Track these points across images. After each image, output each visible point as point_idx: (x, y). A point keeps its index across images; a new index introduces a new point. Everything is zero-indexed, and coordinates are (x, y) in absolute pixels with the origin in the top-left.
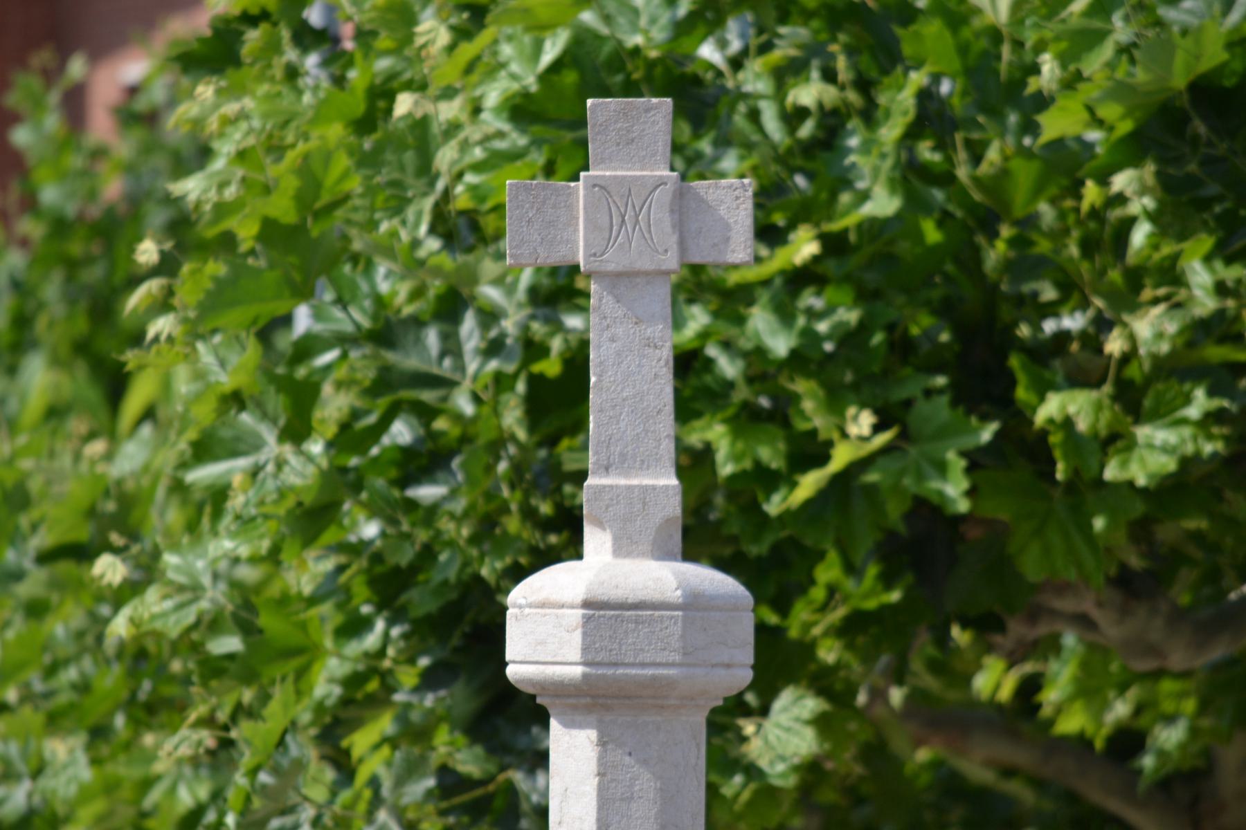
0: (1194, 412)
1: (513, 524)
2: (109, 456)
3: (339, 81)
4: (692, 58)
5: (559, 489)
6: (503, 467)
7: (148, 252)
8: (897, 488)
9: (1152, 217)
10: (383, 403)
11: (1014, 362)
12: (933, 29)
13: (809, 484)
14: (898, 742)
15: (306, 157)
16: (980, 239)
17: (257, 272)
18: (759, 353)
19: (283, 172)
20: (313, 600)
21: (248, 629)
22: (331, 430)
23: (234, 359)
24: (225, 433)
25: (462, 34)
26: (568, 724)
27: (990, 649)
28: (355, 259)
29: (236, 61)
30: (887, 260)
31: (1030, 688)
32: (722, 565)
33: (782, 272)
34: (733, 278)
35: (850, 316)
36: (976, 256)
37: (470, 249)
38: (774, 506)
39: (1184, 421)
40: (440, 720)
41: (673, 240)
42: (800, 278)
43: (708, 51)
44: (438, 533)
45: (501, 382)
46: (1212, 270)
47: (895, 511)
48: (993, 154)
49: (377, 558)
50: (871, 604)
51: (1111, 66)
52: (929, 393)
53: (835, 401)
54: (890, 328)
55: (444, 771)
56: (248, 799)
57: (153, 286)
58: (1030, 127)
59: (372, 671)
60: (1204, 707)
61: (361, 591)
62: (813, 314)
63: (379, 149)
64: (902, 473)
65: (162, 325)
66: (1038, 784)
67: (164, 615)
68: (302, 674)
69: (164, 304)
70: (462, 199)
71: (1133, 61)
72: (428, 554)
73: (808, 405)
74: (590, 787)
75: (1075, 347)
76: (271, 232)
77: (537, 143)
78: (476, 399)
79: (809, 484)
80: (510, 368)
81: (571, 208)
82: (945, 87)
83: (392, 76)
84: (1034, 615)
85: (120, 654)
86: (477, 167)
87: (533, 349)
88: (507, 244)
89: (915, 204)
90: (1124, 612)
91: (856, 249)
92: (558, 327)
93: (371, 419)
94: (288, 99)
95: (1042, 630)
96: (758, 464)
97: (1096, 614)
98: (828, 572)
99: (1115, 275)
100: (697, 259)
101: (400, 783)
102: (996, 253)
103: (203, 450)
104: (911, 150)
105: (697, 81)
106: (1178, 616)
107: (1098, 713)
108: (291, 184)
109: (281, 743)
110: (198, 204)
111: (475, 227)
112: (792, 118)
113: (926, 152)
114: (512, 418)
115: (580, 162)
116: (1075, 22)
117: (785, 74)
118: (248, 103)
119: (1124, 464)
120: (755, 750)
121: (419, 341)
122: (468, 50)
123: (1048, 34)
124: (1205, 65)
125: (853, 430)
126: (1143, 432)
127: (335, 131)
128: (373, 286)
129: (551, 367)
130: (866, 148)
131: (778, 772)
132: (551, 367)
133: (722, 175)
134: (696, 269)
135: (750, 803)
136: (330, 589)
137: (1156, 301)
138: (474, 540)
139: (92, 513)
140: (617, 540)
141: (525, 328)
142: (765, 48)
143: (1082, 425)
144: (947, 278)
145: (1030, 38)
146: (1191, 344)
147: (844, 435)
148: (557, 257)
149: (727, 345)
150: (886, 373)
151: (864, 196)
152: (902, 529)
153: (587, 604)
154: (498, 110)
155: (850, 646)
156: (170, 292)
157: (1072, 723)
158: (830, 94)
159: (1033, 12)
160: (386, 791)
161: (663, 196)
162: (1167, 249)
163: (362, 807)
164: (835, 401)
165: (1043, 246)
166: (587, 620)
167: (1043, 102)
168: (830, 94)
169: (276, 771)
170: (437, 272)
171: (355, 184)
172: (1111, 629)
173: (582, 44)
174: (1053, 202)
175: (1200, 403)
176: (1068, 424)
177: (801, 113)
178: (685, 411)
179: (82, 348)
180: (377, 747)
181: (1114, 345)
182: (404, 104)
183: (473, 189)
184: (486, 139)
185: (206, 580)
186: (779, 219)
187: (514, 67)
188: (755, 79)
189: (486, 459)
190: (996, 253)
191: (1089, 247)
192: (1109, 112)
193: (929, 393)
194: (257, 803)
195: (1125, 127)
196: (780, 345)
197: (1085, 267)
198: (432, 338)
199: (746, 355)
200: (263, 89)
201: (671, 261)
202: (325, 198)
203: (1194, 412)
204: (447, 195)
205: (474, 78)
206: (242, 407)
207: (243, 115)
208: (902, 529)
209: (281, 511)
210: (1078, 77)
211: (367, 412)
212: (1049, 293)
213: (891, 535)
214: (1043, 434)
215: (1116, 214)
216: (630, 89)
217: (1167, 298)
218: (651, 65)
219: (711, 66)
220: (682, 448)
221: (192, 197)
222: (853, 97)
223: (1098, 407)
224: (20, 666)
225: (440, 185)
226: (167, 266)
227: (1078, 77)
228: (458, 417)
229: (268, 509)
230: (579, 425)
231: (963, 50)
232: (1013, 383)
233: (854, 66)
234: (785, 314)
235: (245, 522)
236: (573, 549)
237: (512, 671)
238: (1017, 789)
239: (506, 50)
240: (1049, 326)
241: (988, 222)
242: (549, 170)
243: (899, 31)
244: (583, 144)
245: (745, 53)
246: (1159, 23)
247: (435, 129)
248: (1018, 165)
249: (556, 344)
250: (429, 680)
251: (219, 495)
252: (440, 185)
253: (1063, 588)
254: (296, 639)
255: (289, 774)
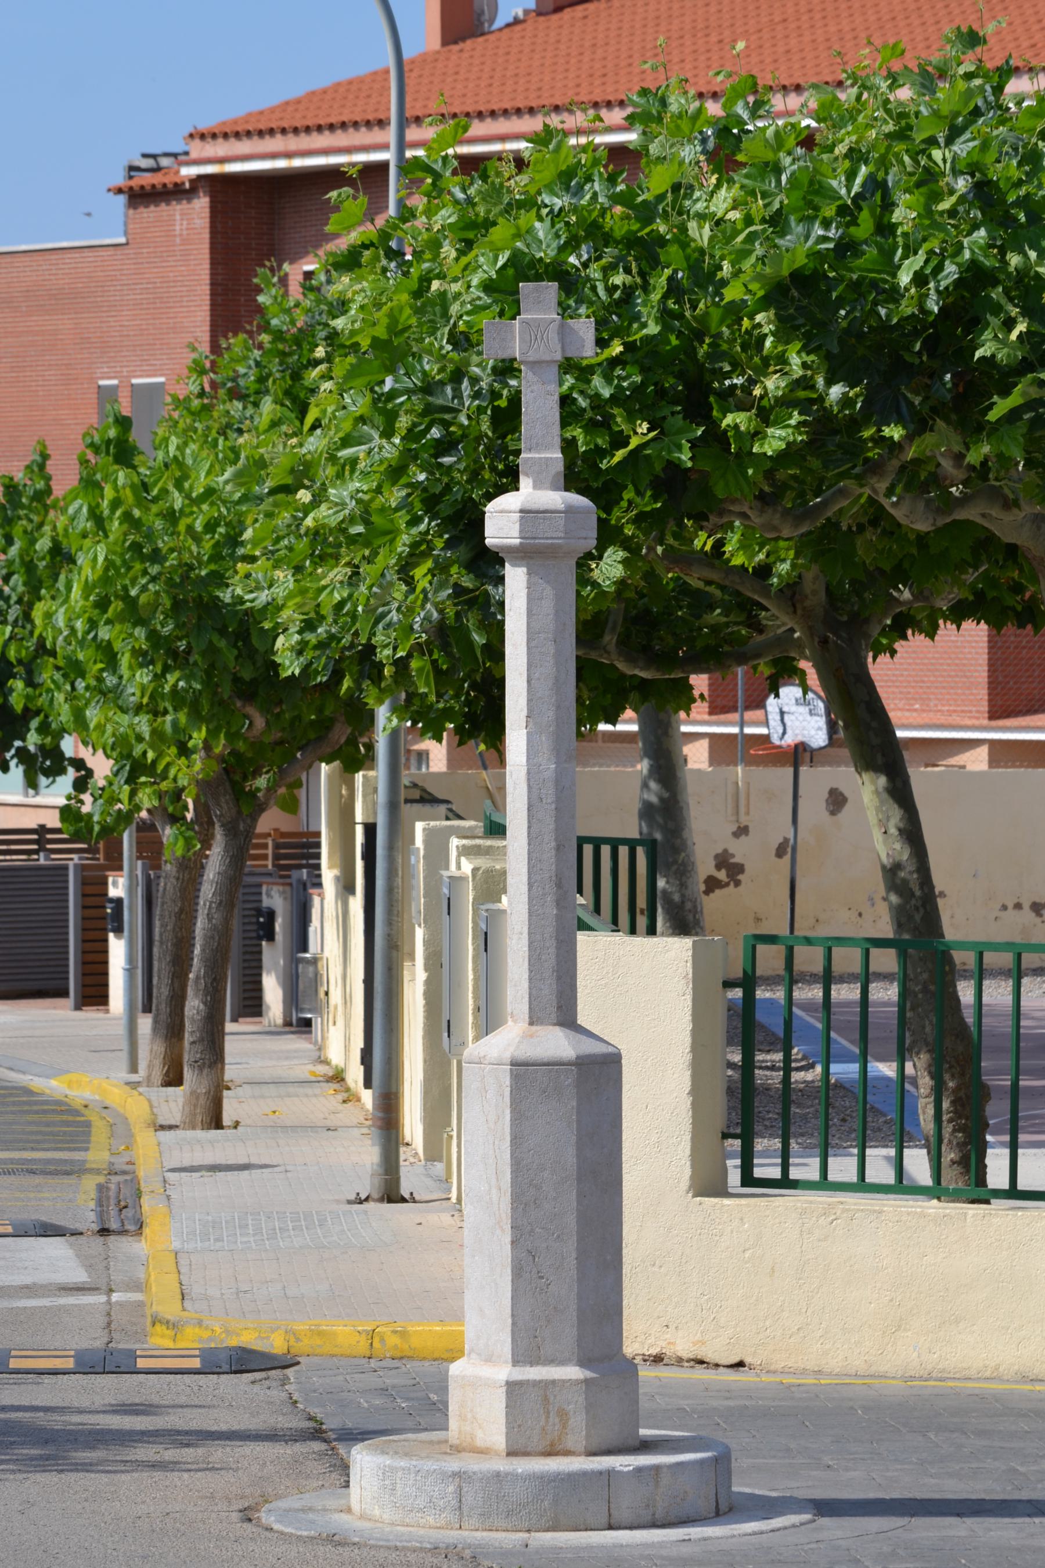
0: (793, 422)
1: (487, 475)
2: (301, 445)
3: (406, 274)
4: (566, 263)
5: (507, 458)
6: (481, 447)
7: (320, 352)
8: (659, 456)
9: (773, 334)
10: (427, 420)
11: (712, 399)
12: (674, 249)
13: (620, 455)
14: (659, 570)
15: (391, 309)
16: (696, 344)
17: (370, 360)
18: (598, 395)
19: (381, 316)
20: (397, 509)
21: (367, 523)
22: (404, 432)
23: (360, 401)
24: (356, 434)
25: (462, 253)
26: (513, 565)
27: (702, 528)
28: (414, 355)
29: (359, 265)
30: (654, 354)
31: (719, 544)
32: (580, 492)
33: (607, 359)
34: (585, 363)
35: (638, 379)
36: (694, 350)
37: (465, 350)
38: (603, 466)
39: (789, 426)
40: (454, 562)
41: (559, 347)
42: (615, 362)
43: (572, 260)
44: (453, 478)
45: (480, 410)
46: (800, 357)
47: (658, 467)
48: (701, 305)
49: (425, 490)
50: (648, 509)
51: (754, 266)
52: (673, 413)
53: (631, 418)
54: (656, 384)
55: (456, 585)
56: (368, 599)
57: (323, 367)
58: (718, 293)
59: (423, 541)
60: (797, 556)
61: (418, 505)
62: (619, 377)
63: (424, 305)
64: (662, 449)
65: (327, 385)
66: (722, 588)
67: (329, 516)
68: (392, 541)
69: (327, 377)
70: (462, 326)
71: (764, 264)
72: (448, 488)
73: (619, 420)
74: (524, 593)
75: (738, 392)
76: (376, 343)
77: (495, 301)
78: (469, 417)
79: (620, 455)
80: (485, 404)
81: (513, 332)
82: (680, 275)
83: (430, 271)
84: (721, 513)
85: (306, 534)
86: (468, 313)
87: (495, 395)
88: (484, 347)
89: (666, 328)
90: (762, 512)
91: (640, 348)
92: (507, 385)
93: (423, 427)
94: (382, 283)
95: (725, 520)
96: (596, 445)
97: (749, 513)
98: (628, 494)
99: (757, 359)
100: (569, 355)
101: (436, 592)
102: (703, 350)
103: (346, 442)
104: (664, 304)
105: (568, 273)
106: (786, 513)
107: (751, 558)
108: (385, 321)
109: (383, 575)
110: (343, 330)
111: (468, 339)
112: (611, 289)
113: (671, 304)
114: (485, 426)
115: (515, 310)
116: (738, 246)
117: (608, 270)
118: (365, 284)
119: (762, 446)
120: (596, 574)
121: (443, 392)
122: (464, 260)
123: (726, 252)
124: (796, 266)
125: (639, 431)
126: (770, 431)
127: (404, 297)
128: (422, 367)
129: (503, 403)
130: (645, 304)
131: (607, 585)
132: (503, 403)
133: (580, 316)
134: (568, 359)
135: (594, 599)
136: (405, 504)
137: (776, 372)
138: (468, 481)
139: (292, 471)
140: (534, 482)
141: (491, 385)
142: (598, 258)
143: (743, 428)
144: (680, 360)
145: (718, 254)
146: (791, 391)
147: (636, 433)
148: (506, 355)
149: (582, 392)
150: (653, 404)
151: (644, 325)
152: (662, 475)
153: (521, 511)
154: (477, 287)
155: (638, 528)
156: (330, 369)
157: (737, 561)
158: (628, 279)
159: (719, 242)
160: (430, 595)
161: (554, 327)
162: (780, 349)
163: (419, 603)
164: (631, 418)
165: (725, 347)
166: (522, 518)
167: (724, 283)
168: (628, 279)
169: (380, 586)
170: (451, 361)
171: (413, 321)
172: (756, 519)
173: (515, 258)
174: (728, 327)
175: (796, 418)
176: (736, 427)
177: (616, 287)
178: (564, 423)
179: (287, 393)
180: (425, 575)
181: (757, 392)
182: (435, 285)
183: (467, 323)
184: (473, 300)
185: (348, 501)
186: (605, 336)
187: (485, 267)
188: (594, 272)
189: (474, 445)
190: (703, 350)
191: (745, 347)
192: (754, 286)
193: (673, 413)
194: (372, 601)
195: (761, 293)
196: (606, 393)
197: (743, 355)
198: (449, 390)
199: (590, 397)
200: (371, 277)
201: (558, 356)
202: (400, 327)
203: (793, 422)
204: (455, 325)
205: (467, 273)
206: (365, 423)
207: (363, 290)
208: (662, 475)
209: (382, 469)
210: (740, 271)
211: (421, 424)
212: (727, 368)
213: (657, 477)
214: (725, 432)
215: (756, 332)
216: (538, 278)
217: (781, 370)
218: (547, 265)
219: (575, 266)
220: (564, 440)
221: (340, 327)
222: (638, 280)
223: (750, 420)
224: (263, 540)
225: (452, 321)
226: (329, 359)
227: (740, 271)
228: (461, 426)
229: (374, 468)
230: (516, 428)
231: (687, 258)
232: (712, 409)
233: (639, 266)
234: (608, 379)
235: (365, 474)
236: (514, 485)
237: (487, 541)
238: (711, 589)
239: (481, 259)
240: (727, 382)
241: (699, 335)
242: (501, 314)
243: (659, 250)
244: (518, 302)
245: (589, 260)
246: (776, 246)
247: (449, 296)
248: (712, 310)
249: (505, 392)
250: (449, 545)
251: (354, 462)
252: (452, 321)
253: (734, 501)
254: (389, 526)
255: (387, 588)
